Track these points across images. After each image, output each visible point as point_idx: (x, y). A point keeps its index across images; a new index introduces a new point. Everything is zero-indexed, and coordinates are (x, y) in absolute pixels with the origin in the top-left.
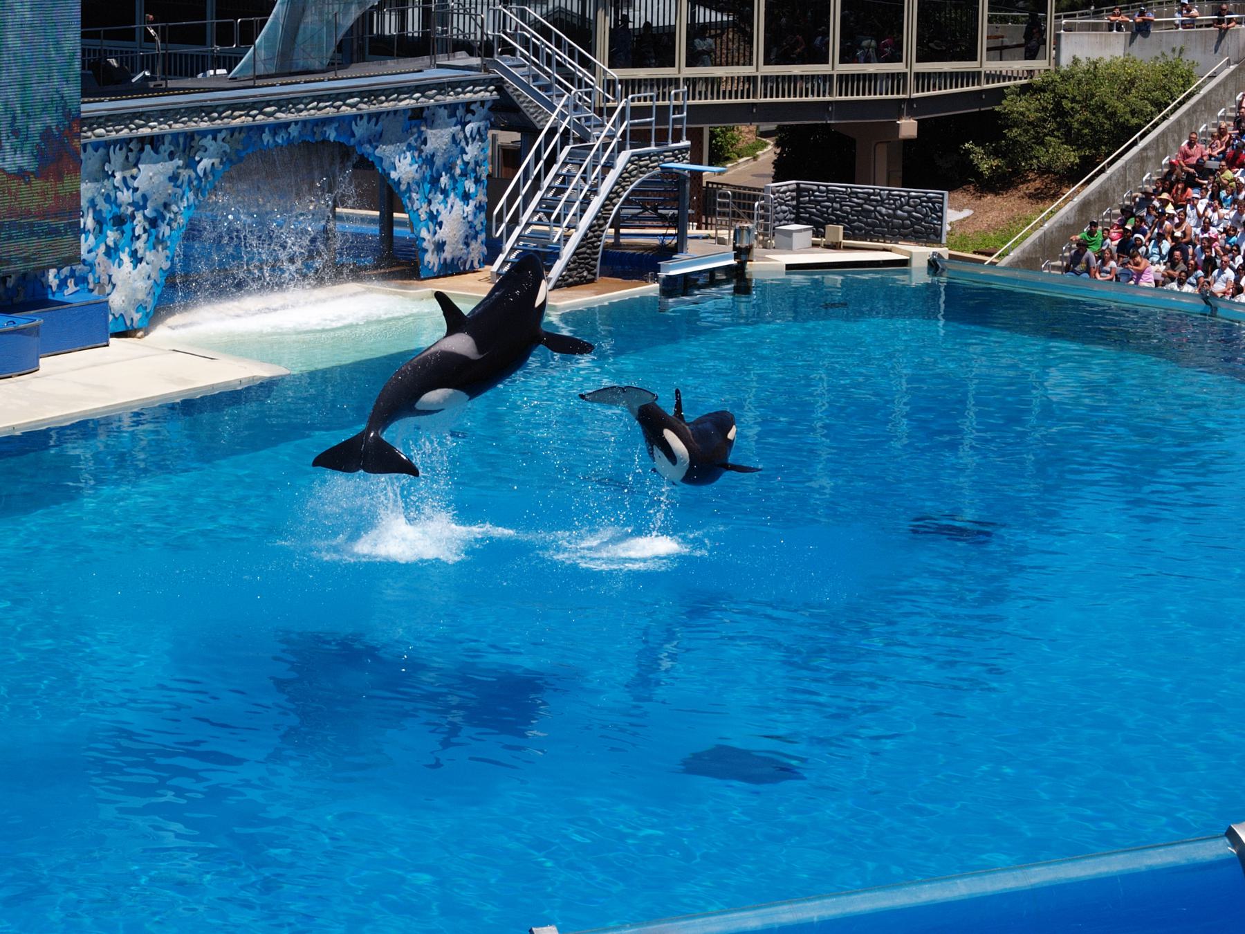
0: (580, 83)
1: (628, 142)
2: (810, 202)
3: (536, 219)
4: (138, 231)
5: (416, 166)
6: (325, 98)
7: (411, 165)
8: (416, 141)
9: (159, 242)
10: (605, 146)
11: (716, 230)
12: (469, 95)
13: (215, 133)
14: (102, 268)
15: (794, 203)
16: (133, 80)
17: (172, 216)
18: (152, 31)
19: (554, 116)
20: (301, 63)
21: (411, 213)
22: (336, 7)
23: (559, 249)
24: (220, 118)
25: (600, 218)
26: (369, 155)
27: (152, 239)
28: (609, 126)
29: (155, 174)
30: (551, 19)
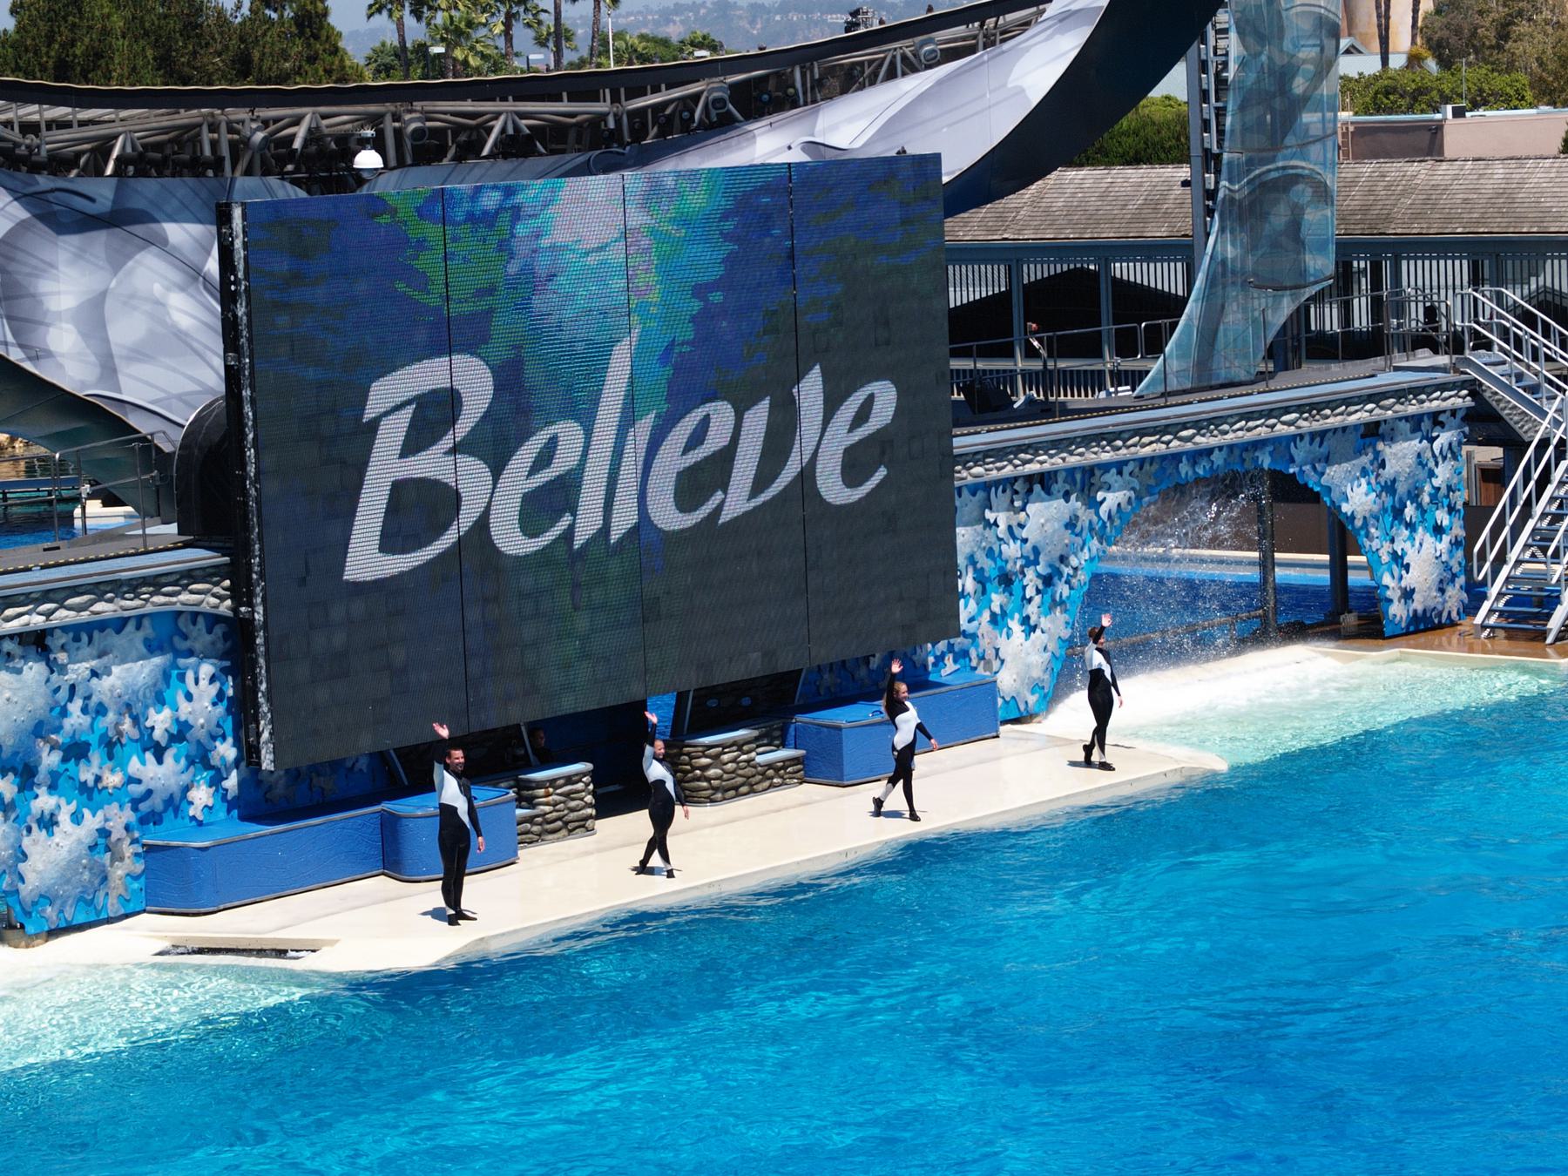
3: (1527, 555)
4: (1030, 592)
7: (1367, 494)
9: (1056, 603)
12: (1435, 403)
13: (1120, 466)
14: (987, 640)
16: (1016, 406)
17: (1071, 572)
18: (1036, 344)
19: (1545, 423)
20: (1223, 375)
21: (1369, 555)
23: (1559, 591)
27: (1048, 598)
29: (1047, 521)
30: (1534, 301)
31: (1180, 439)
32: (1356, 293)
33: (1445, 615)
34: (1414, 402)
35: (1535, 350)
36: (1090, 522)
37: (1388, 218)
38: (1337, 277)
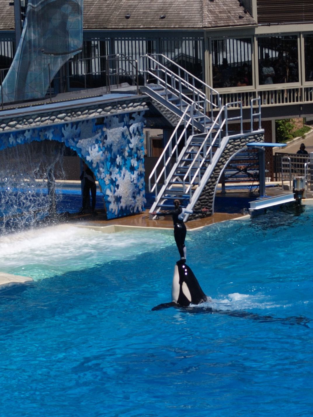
0: (197, 98)
1: (227, 131)
3: (174, 180)
5: (101, 152)
6: (45, 115)
7: (98, 152)
10: (213, 135)
11: (283, 181)
12: (130, 108)
19: (182, 118)
20: (30, 94)
21: (100, 180)
22: (49, 60)
23: (189, 197)
25: (213, 177)
28: (215, 122)
30: (177, 60)
31: (10, 126)
32: (93, 56)
33: (136, 209)
34: (120, 108)
35: (177, 83)
37: (108, 21)
38: (84, 48)
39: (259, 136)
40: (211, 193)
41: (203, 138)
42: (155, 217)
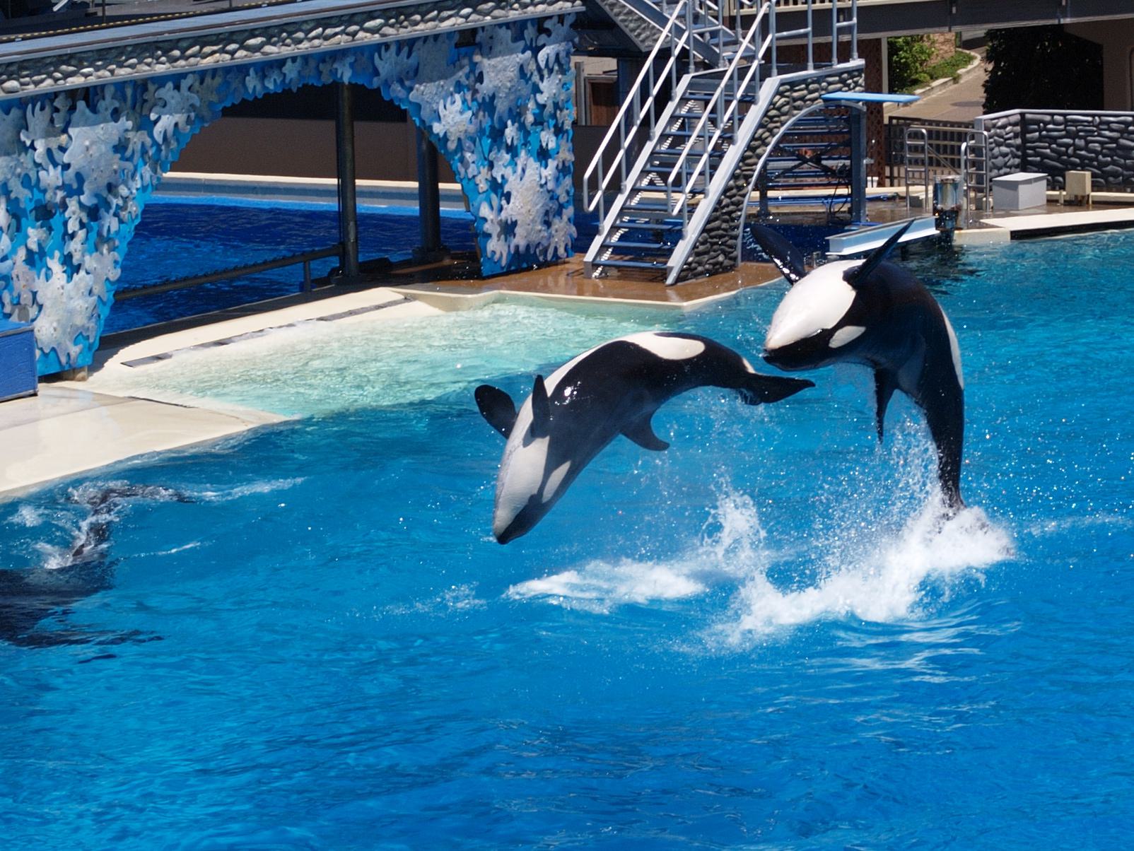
1: (774, 64)
2: (1041, 139)
3: (645, 182)
4: (72, 226)
5: (469, 113)
6: (334, 21)
7: (461, 113)
8: (468, 78)
9: (101, 241)
10: (742, 72)
11: (907, 185)
13: (177, 80)
14: (22, 283)
15: (1019, 141)
16: (55, 9)
17: (121, 202)
19: (665, 32)
21: (465, 182)
23: (682, 224)
24: (184, 57)
26: (400, 100)
27: (93, 235)
28: (745, 43)
29: (93, 143)
31: (248, 48)
33: (551, 251)
36: (143, 144)
39: (852, 78)
40: (734, 215)
41: (716, 81)
42: (596, 274)
